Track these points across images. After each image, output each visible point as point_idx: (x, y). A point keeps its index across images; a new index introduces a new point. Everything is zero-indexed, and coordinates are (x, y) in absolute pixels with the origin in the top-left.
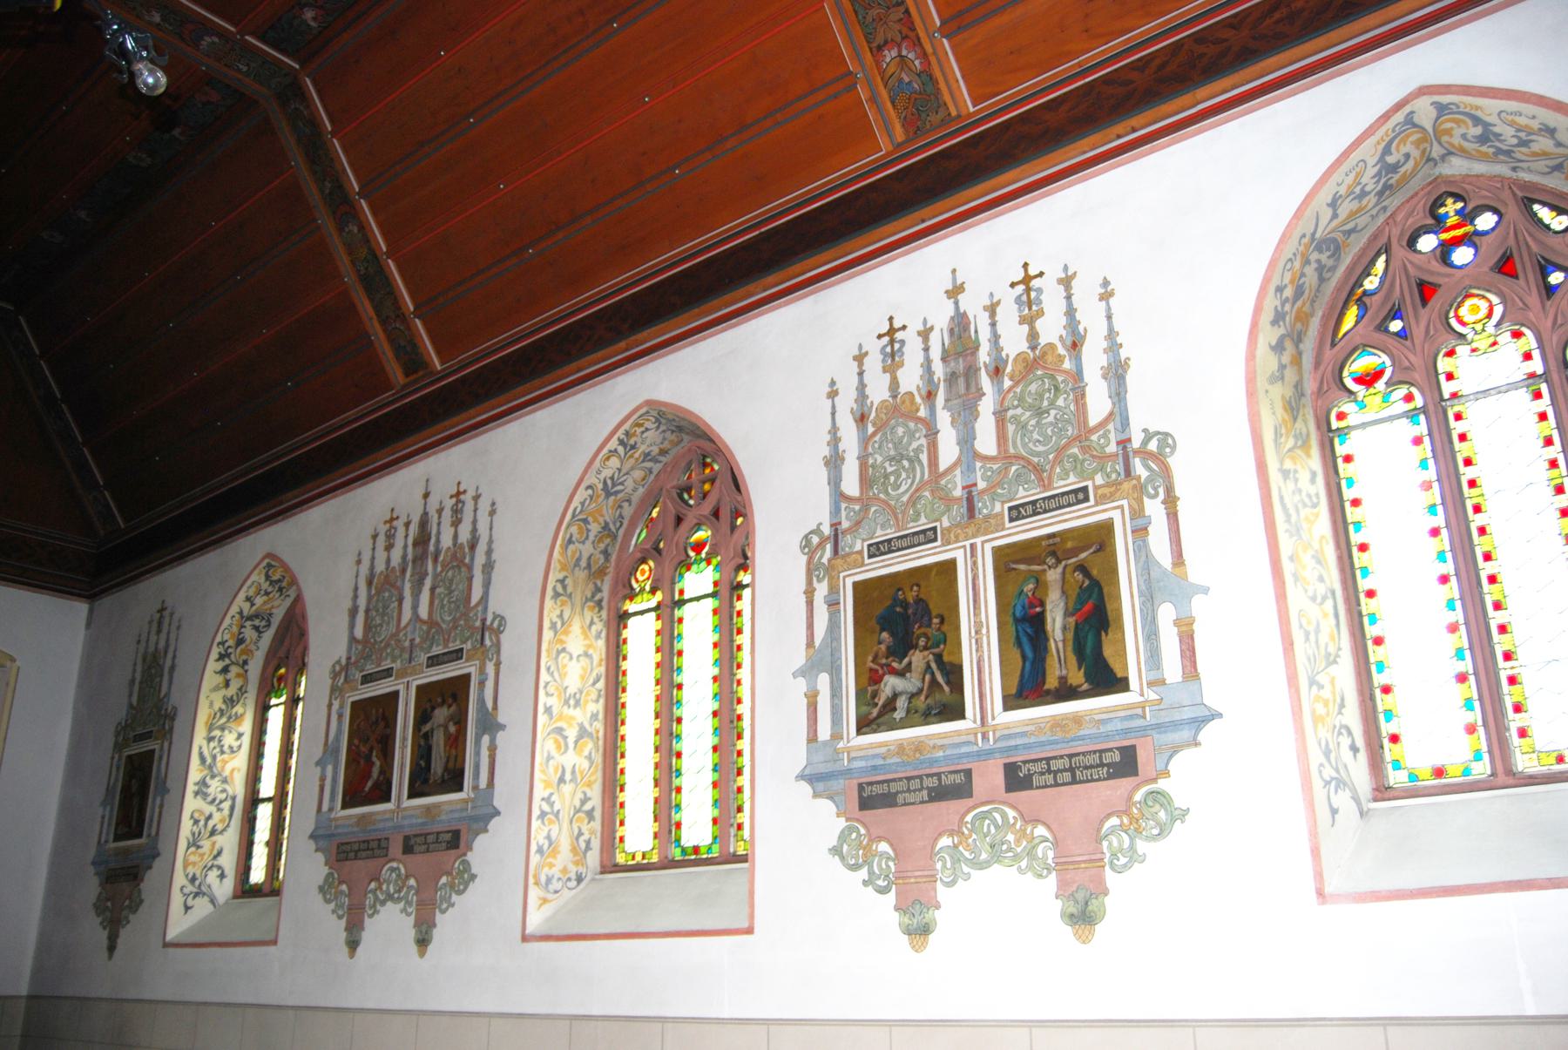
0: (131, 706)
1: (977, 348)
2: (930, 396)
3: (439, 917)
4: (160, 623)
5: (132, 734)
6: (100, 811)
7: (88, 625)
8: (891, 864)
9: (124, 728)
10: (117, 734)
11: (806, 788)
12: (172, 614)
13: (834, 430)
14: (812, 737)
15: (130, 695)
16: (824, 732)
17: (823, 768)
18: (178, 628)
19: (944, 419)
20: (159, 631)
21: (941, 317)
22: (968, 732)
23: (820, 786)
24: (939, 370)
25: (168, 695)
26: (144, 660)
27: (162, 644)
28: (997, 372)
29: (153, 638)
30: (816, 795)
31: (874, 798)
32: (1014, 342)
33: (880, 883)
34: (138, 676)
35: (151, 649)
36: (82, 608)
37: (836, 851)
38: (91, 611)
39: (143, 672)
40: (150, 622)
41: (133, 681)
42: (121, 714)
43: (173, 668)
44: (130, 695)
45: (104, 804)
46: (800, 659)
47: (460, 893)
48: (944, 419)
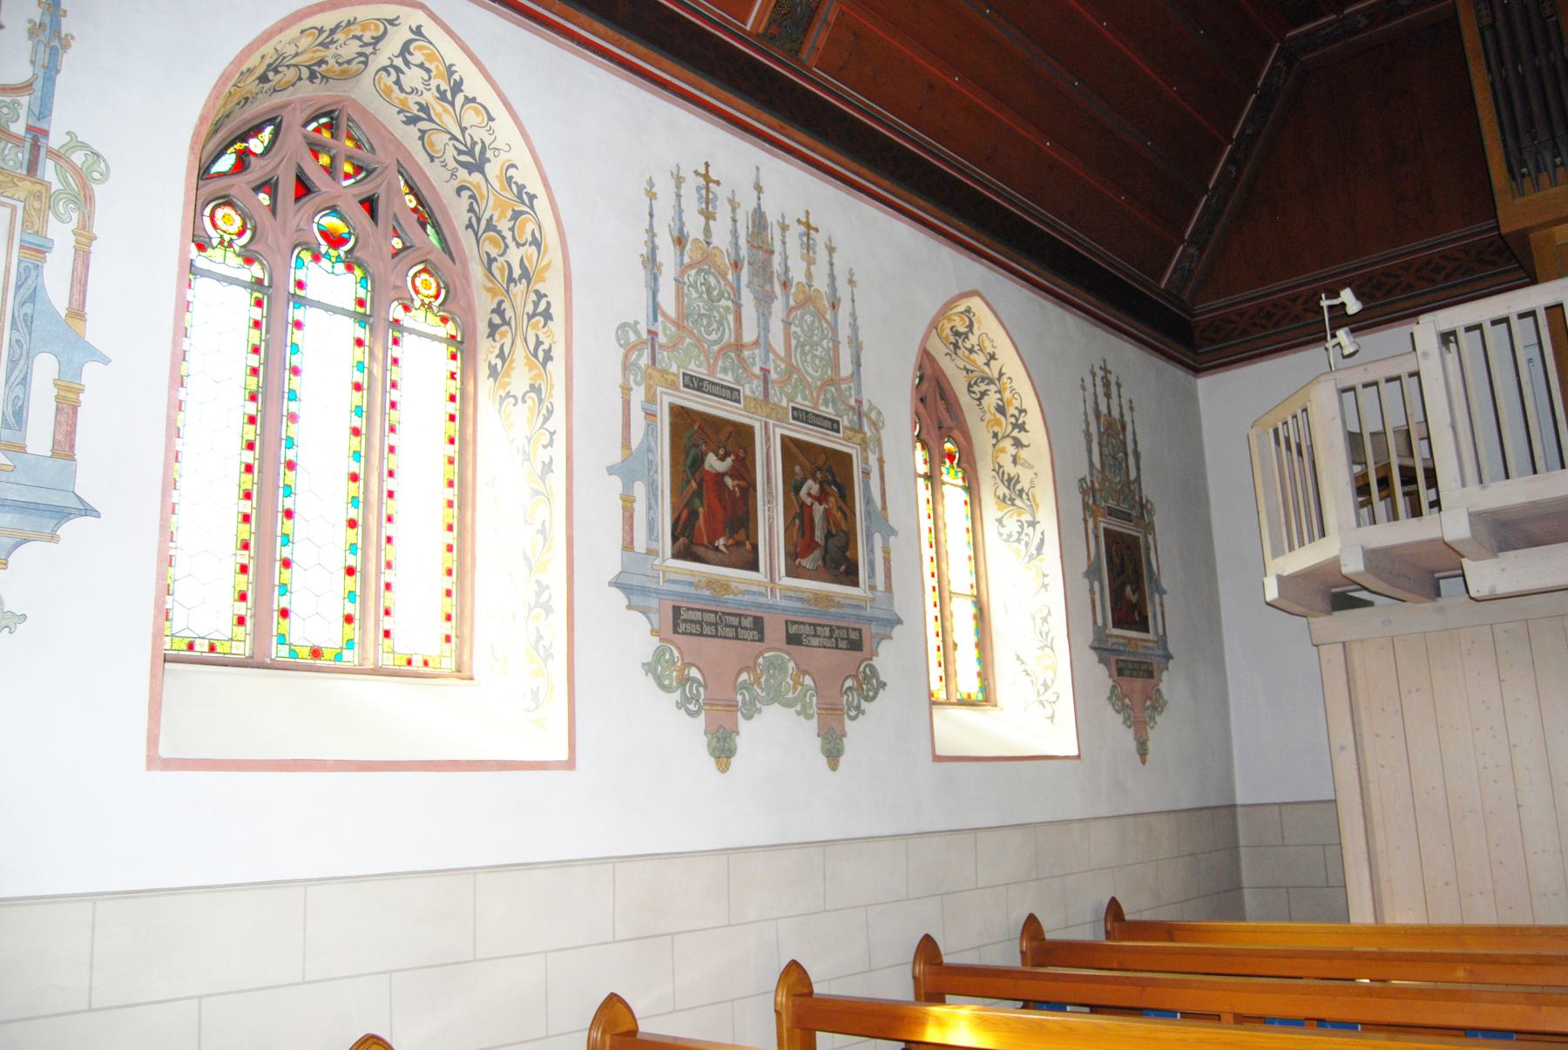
1: (772, 252)
2: (736, 265)
3: (849, 725)
8: (701, 690)
11: (619, 598)
13: (651, 231)
14: (628, 545)
16: (640, 543)
17: (637, 581)
19: (747, 298)
21: (748, 204)
22: (759, 583)
23: (636, 599)
24: (744, 252)
28: (785, 285)
30: (629, 607)
31: (685, 621)
32: (797, 274)
33: (692, 707)
37: (649, 668)
46: (616, 456)
47: (868, 699)
48: (747, 298)
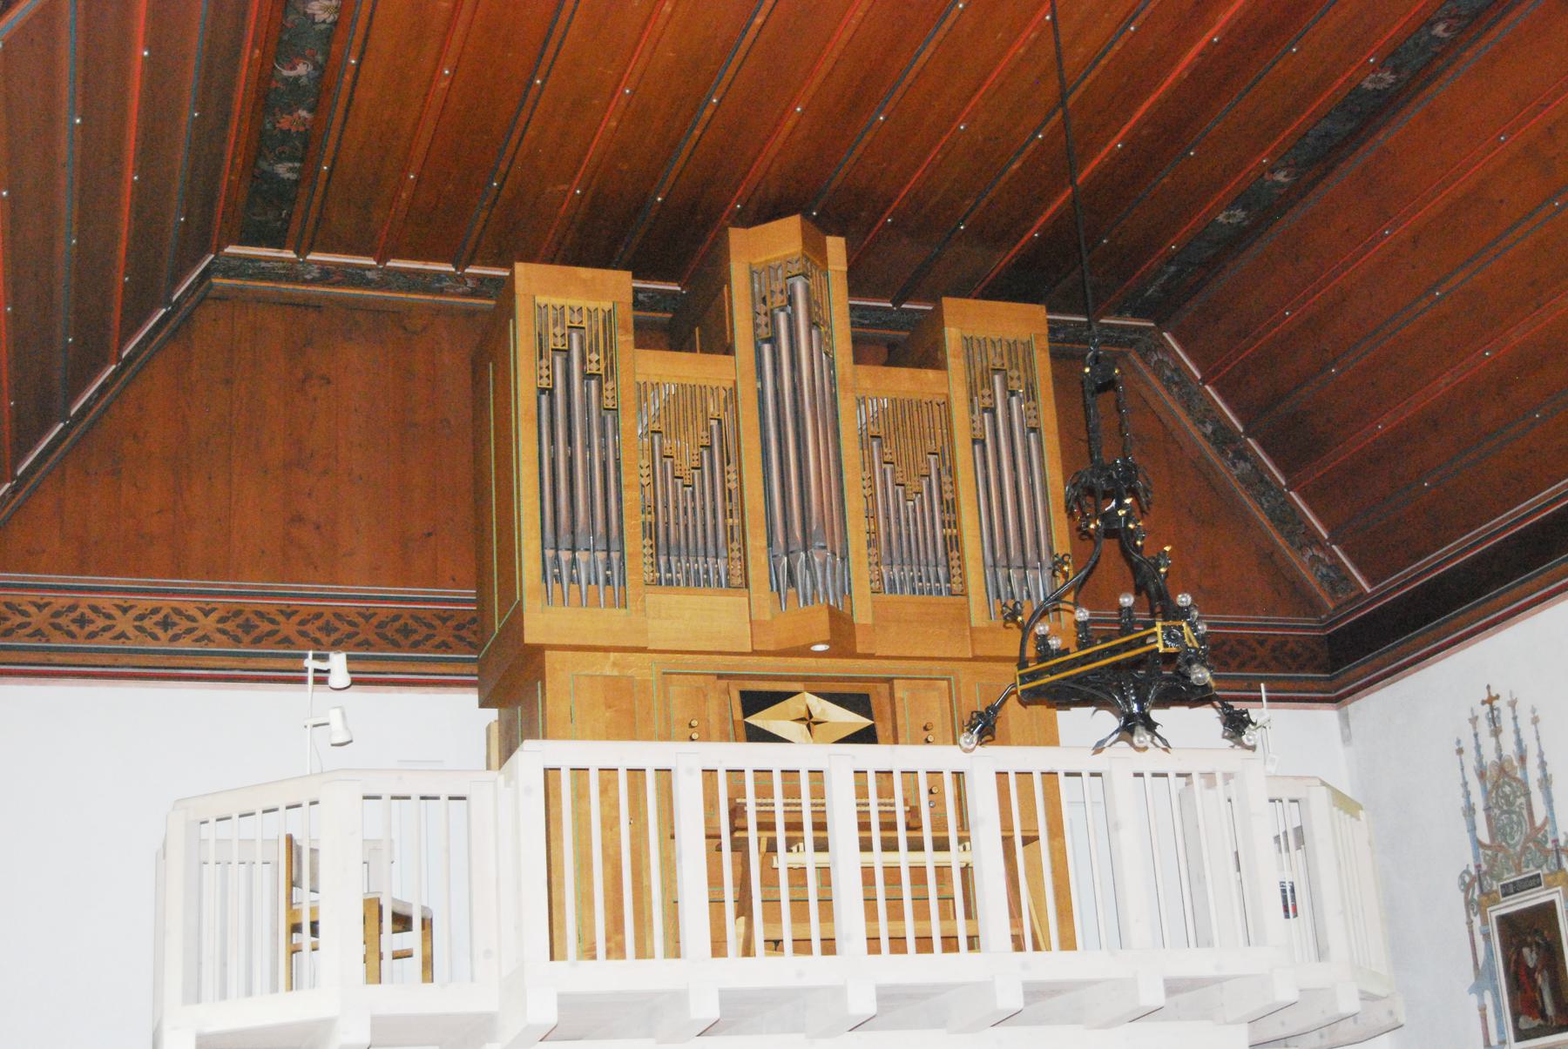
0: (1478, 844)
4: (1494, 720)
5: (1496, 886)
6: (1474, 998)
7: (1347, 739)
9: (1479, 878)
10: (1467, 888)
12: (1513, 704)
15: (1473, 829)
18: (1535, 721)
20: (1496, 732)
25: (1550, 818)
26: (1482, 775)
27: (1509, 749)
29: (1488, 744)
34: (1478, 800)
35: (1490, 757)
36: (1324, 717)
38: (1345, 720)
39: (1487, 794)
40: (1474, 720)
41: (1470, 810)
42: (1465, 858)
43: (1545, 782)
44: (1473, 829)
45: (1477, 989)
